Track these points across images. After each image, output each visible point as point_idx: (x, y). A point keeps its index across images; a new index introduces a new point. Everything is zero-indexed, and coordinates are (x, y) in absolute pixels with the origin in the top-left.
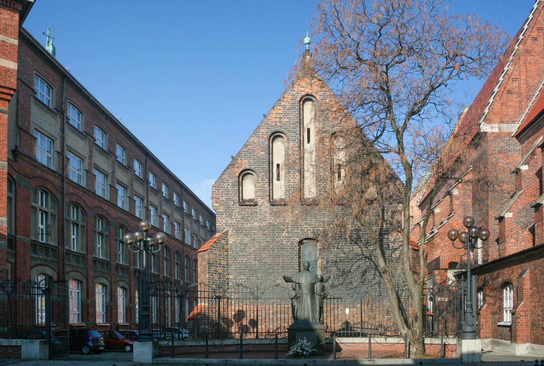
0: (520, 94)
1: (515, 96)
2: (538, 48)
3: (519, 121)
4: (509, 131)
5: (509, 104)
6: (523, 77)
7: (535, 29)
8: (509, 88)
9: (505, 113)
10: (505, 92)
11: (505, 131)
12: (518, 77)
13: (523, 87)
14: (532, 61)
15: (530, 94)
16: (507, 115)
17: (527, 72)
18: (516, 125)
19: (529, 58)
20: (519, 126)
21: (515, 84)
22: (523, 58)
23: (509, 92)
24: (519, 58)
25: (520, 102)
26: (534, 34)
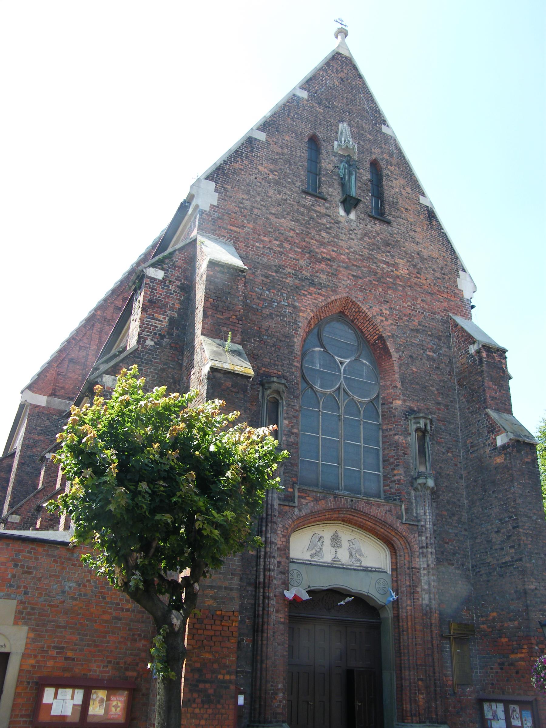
1: (78, 367)
8: (73, 355)
9: (60, 385)
10: (67, 360)
16: (62, 388)
19: (107, 327)
21: (83, 353)
22: (98, 326)
24: (93, 325)
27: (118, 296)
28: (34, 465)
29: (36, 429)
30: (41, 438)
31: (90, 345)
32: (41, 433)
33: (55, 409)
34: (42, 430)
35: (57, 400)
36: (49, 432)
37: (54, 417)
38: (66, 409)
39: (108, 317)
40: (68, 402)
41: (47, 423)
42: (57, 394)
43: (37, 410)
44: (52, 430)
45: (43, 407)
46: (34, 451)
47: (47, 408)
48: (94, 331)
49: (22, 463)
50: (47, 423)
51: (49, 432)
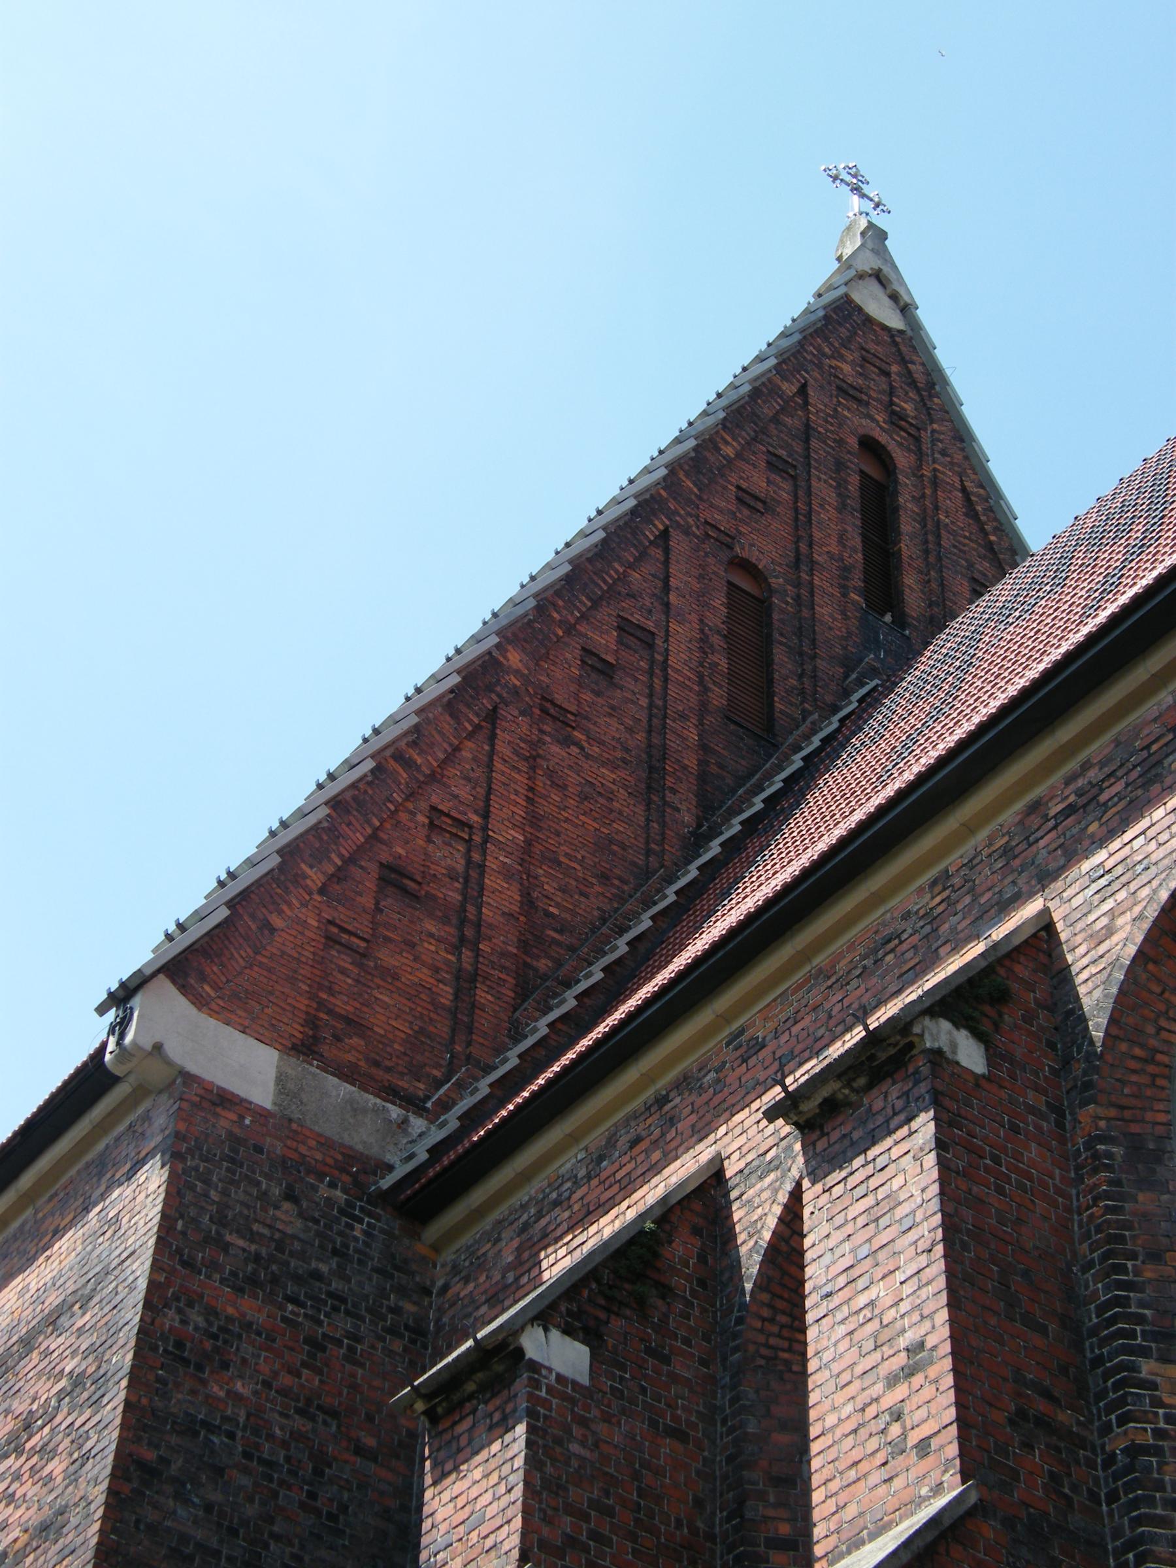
0: (467, 930)
1: (430, 926)
2: (611, 729)
3: (445, 1106)
4: (363, 1137)
5: (386, 957)
6: (507, 833)
7: (607, 614)
9: (342, 1004)
11: (329, 1129)
12: (475, 818)
13: (500, 896)
14: (573, 778)
15: (543, 964)
17: (534, 820)
18: (418, 1124)
19: (555, 749)
20: (437, 1135)
23: (394, 878)
24: (492, 716)
25: (465, 982)
26: (605, 641)
27: (596, 603)
28: (216, 1497)
29: (226, 1247)
30: (253, 1309)
31: (486, 815)
32: (253, 1281)
33: (326, 1144)
34: (257, 1258)
35: (344, 1090)
36: (297, 1278)
37: (324, 1191)
38: (390, 1158)
39: (559, 698)
40: (395, 1112)
41: (287, 1218)
42: (324, 1049)
43: (225, 1121)
44: (317, 1275)
45: (261, 1114)
46: (217, 1390)
47: (281, 1121)
48: (502, 748)
49: (141, 1465)
50: (287, 1218)
51: (297, 1278)
